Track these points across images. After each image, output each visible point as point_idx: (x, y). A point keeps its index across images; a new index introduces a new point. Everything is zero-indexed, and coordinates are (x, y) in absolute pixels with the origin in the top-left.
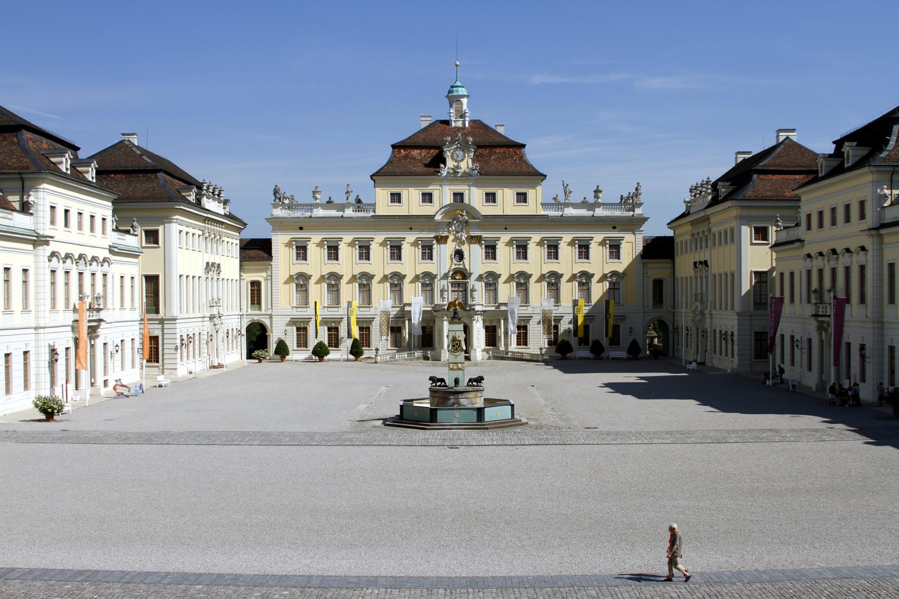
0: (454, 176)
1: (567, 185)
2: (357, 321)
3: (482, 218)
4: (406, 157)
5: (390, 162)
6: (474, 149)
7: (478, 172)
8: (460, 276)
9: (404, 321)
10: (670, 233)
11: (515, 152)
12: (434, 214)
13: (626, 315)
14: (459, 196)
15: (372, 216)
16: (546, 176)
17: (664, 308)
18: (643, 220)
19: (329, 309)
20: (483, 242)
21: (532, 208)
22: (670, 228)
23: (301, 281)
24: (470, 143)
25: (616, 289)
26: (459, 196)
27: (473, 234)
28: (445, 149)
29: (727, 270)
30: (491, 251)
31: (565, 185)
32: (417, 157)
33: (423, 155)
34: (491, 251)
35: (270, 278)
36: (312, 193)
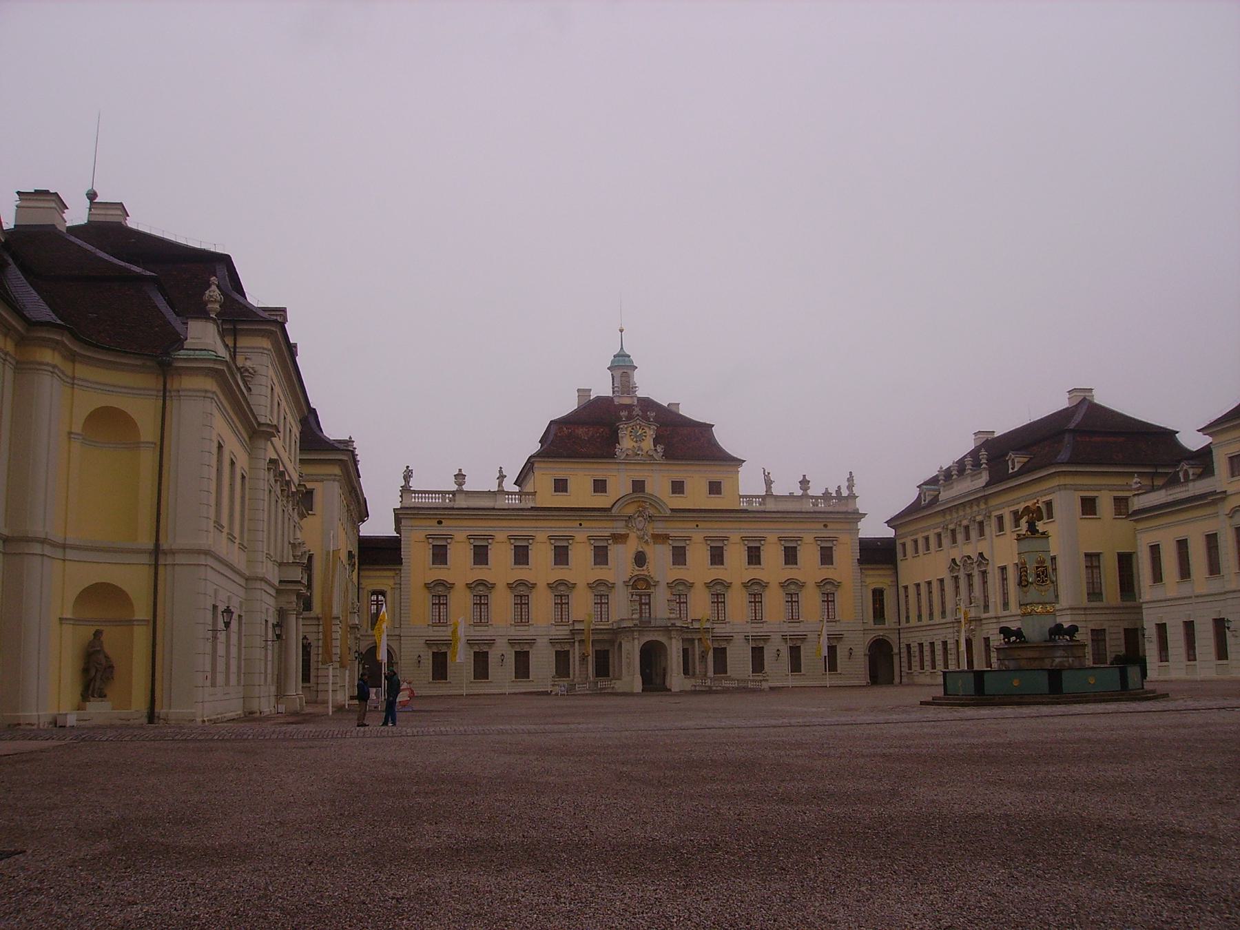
0: (633, 459)
1: (769, 473)
2: (828, 638)
3: (668, 513)
6: (657, 426)
7: (663, 456)
8: (641, 586)
9: (574, 642)
10: (890, 533)
11: (701, 433)
12: (610, 507)
13: (843, 633)
14: (638, 486)
15: (532, 507)
17: (887, 625)
18: (857, 516)
19: (477, 628)
20: (670, 542)
22: (891, 527)
23: (439, 592)
24: (652, 420)
25: (720, 602)
26: (638, 486)
27: (657, 532)
28: (622, 426)
29: (933, 578)
30: (679, 556)
31: (766, 474)
32: (583, 437)
34: (679, 556)
35: (398, 586)
36: (454, 477)
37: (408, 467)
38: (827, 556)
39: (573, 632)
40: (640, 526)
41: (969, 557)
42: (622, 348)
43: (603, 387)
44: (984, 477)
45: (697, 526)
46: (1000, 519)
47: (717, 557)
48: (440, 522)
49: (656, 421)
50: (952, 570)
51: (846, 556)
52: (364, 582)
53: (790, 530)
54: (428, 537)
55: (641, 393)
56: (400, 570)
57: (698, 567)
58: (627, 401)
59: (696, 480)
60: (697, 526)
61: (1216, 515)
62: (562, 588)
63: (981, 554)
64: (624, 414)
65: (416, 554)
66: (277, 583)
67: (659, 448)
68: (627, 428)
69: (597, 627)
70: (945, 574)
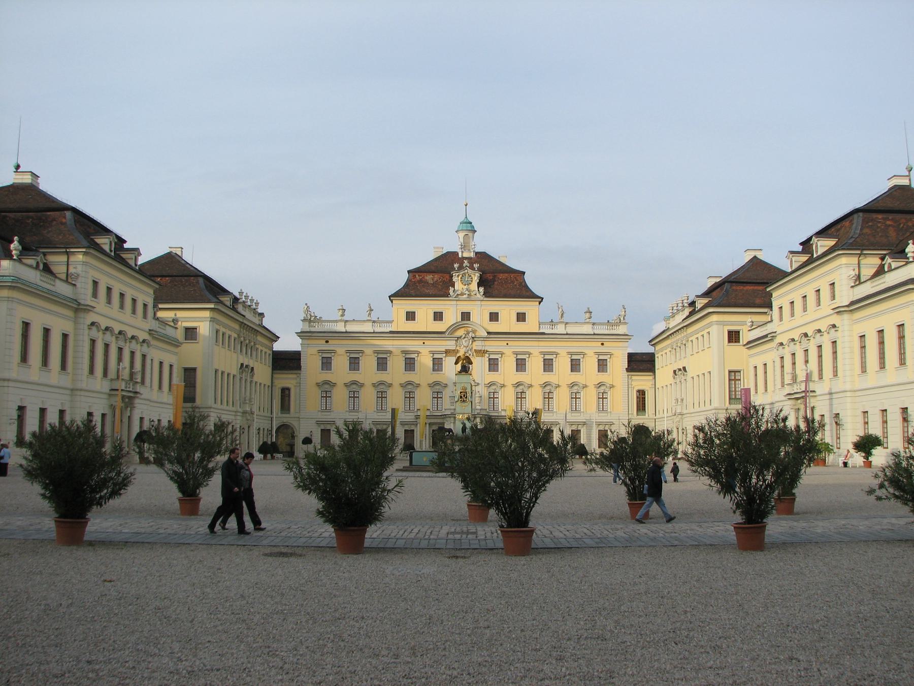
4: (420, 281)
5: (407, 285)
14: (466, 316)
15: (391, 332)
16: (542, 299)
21: (530, 325)
26: (466, 316)
30: (493, 365)
33: (435, 279)
34: (493, 365)
35: (298, 385)
37: (306, 304)
38: (602, 365)
39: (417, 417)
40: (465, 344)
41: (680, 370)
42: (466, 217)
43: (452, 243)
44: (687, 312)
45: (507, 344)
46: (692, 341)
47: (521, 365)
48: (327, 342)
49: (479, 270)
50: (674, 378)
51: (619, 363)
52: (276, 382)
53: (576, 346)
54: (320, 351)
55: (479, 249)
56: (300, 374)
57: (507, 371)
58: (466, 255)
59: (508, 309)
60: (507, 344)
61: (771, 349)
62: (410, 387)
63: (684, 368)
64: (456, 266)
65: (311, 363)
66: (108, 391)
67: (482, 289)
68: (458, 276)
69: (434, 414)
70: (672, 381)
